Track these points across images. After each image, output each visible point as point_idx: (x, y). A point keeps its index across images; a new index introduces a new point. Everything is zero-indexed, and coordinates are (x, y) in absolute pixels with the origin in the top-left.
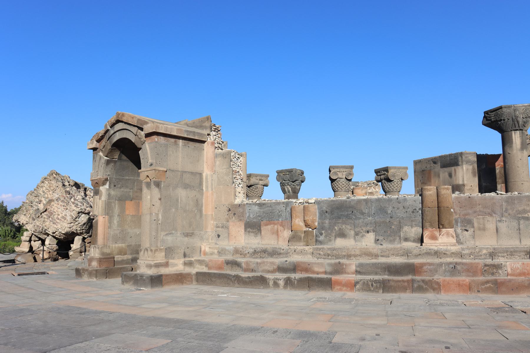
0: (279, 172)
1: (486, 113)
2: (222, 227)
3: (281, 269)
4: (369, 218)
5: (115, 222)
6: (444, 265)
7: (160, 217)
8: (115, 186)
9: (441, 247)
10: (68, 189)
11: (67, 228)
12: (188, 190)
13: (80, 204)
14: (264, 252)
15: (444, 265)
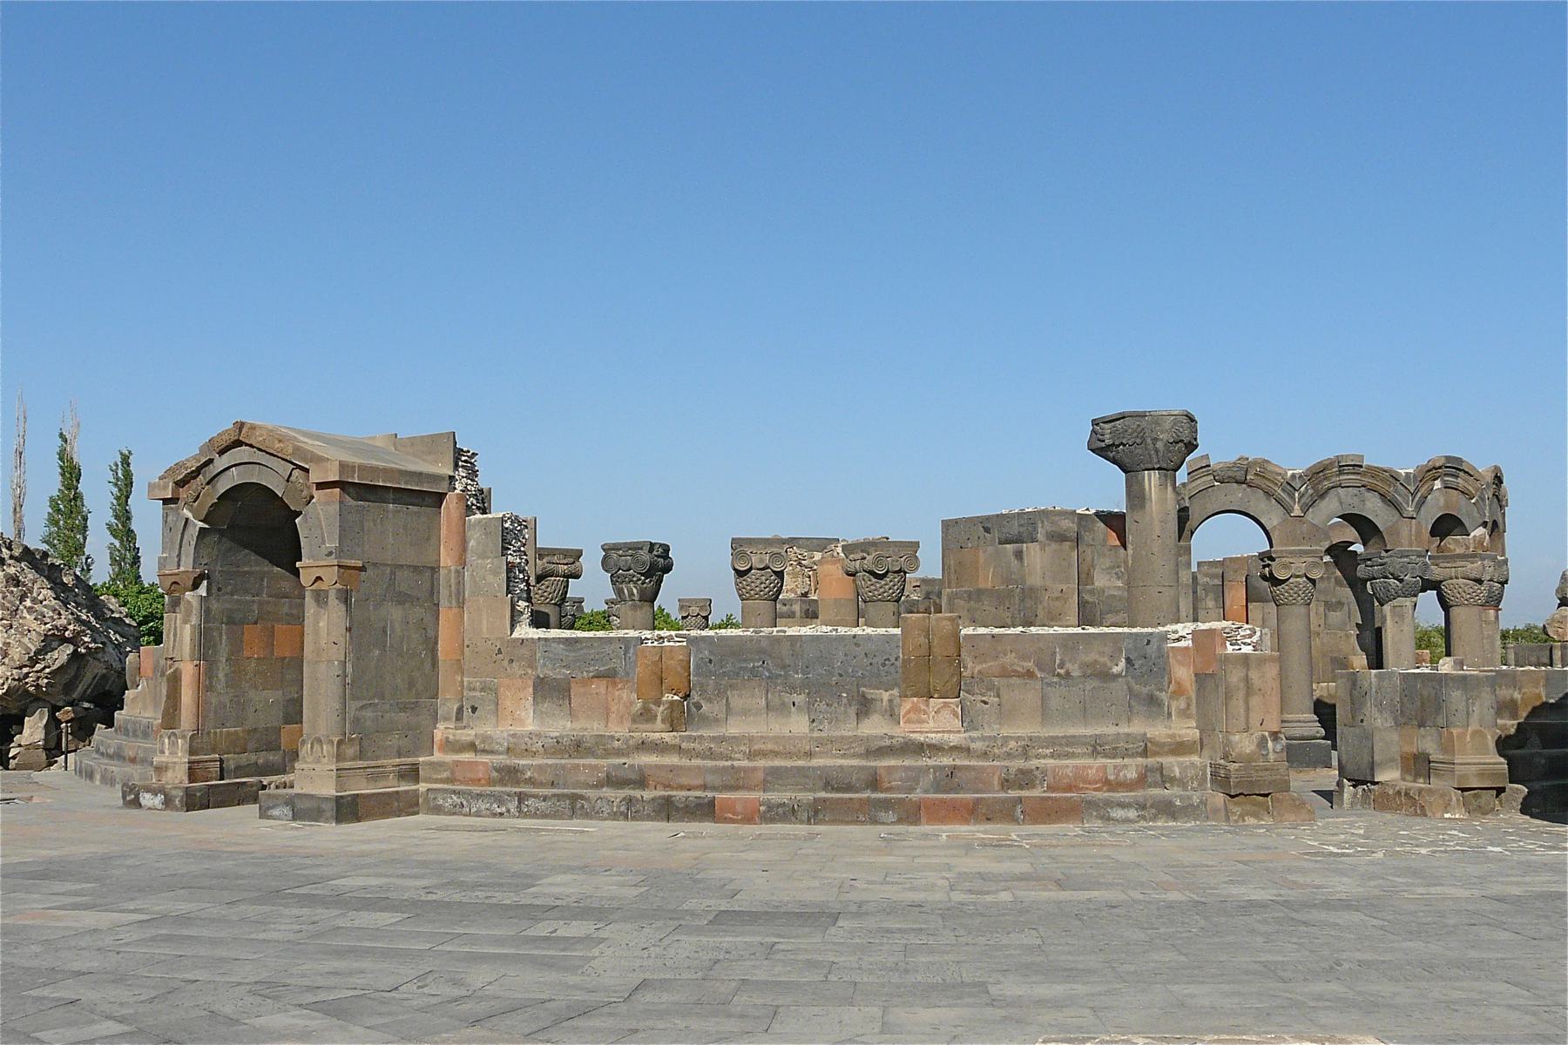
0: (607, 549)
1: (1095, 423)
2: (482, 690)
3: (613, 781)
4: (796, 676)
5: (221, 675)
6: (932, 770)
7: (349, 669)
8: (219, 589)
9: (933, 735)
10: (12, 570)
11: (10, 681)
12: (407, 605)
13: (51, 614)
14: (578, 747)
15: (932, 770)
